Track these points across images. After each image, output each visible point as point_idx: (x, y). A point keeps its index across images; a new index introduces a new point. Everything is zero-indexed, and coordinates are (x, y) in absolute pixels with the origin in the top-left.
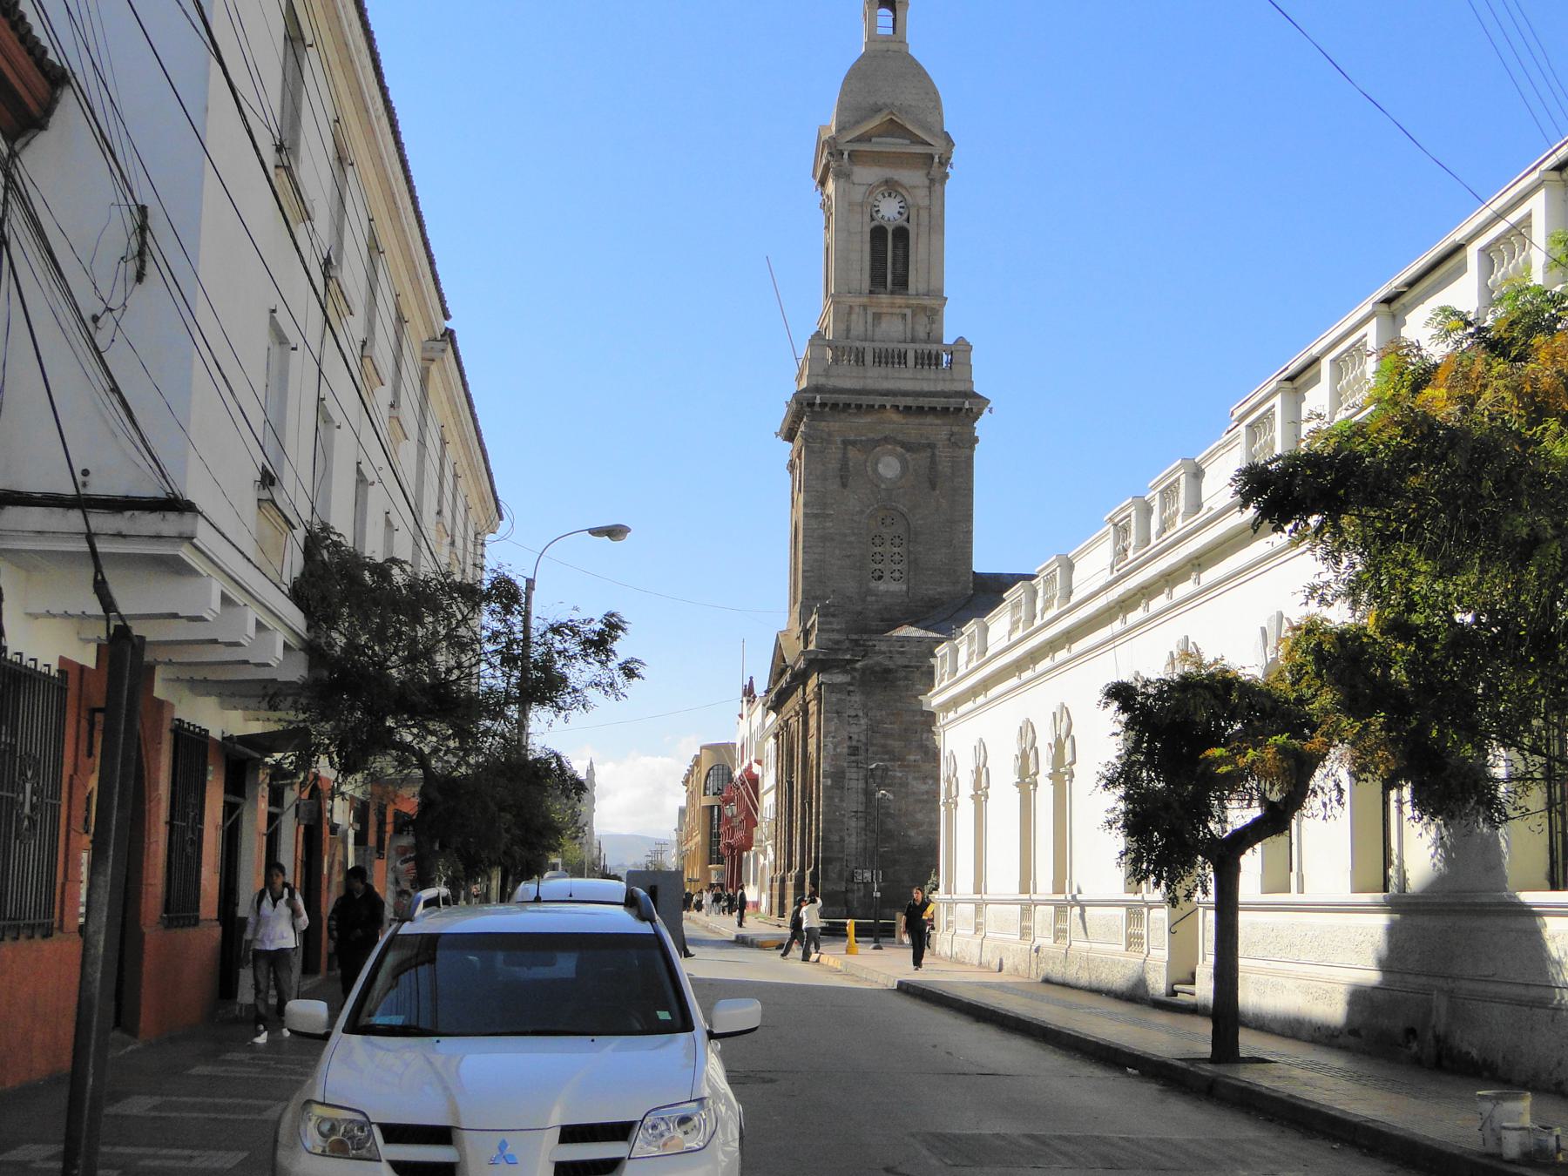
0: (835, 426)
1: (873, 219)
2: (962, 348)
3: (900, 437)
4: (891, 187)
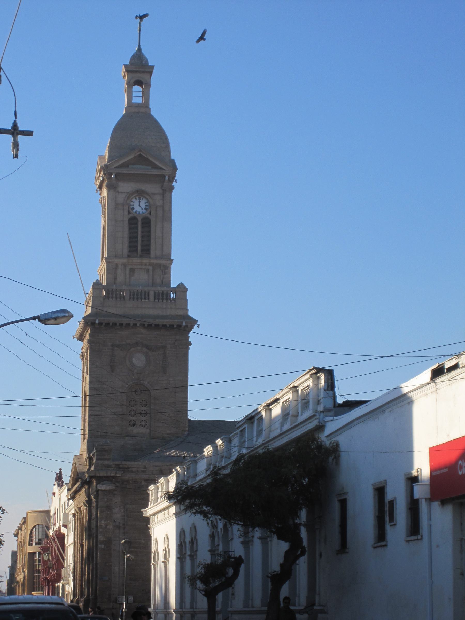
1: (129, 213)
2: (182, 289)
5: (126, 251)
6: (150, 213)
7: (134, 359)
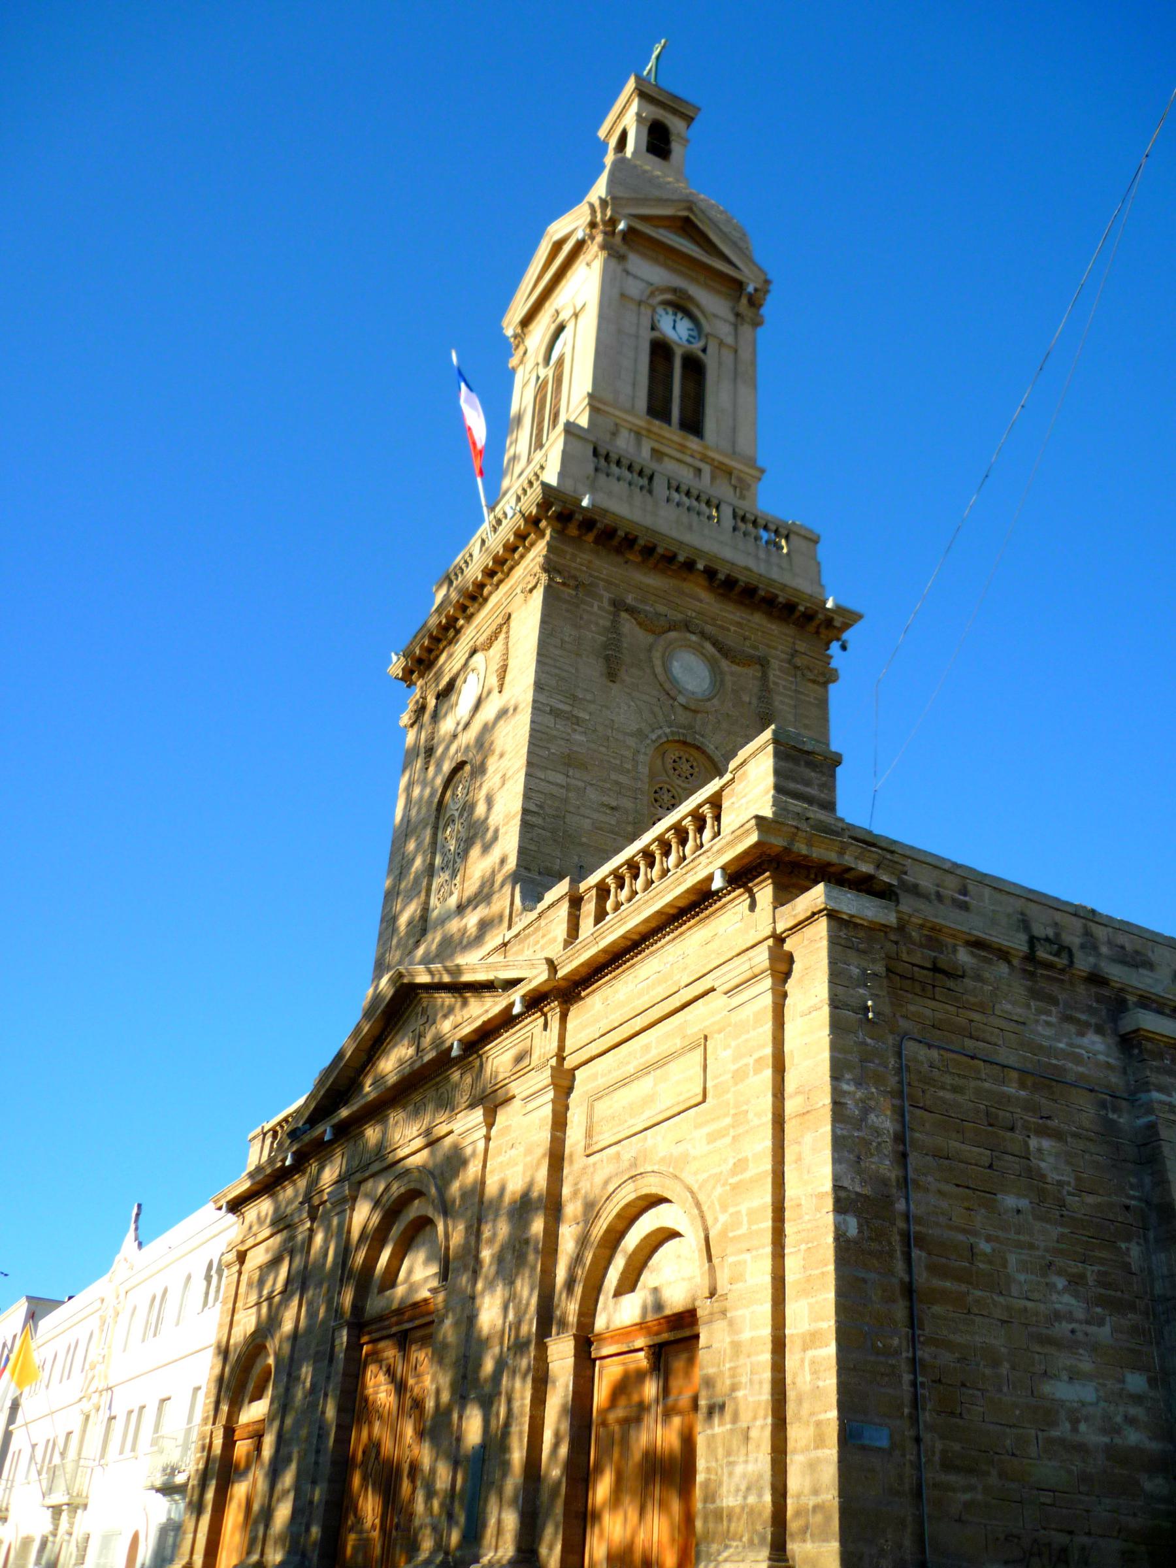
1: (653, 328)
3: (709, 629)
4: (681, 306)
5: (642, 403)
6: (704, 350)
7: (675, 664)
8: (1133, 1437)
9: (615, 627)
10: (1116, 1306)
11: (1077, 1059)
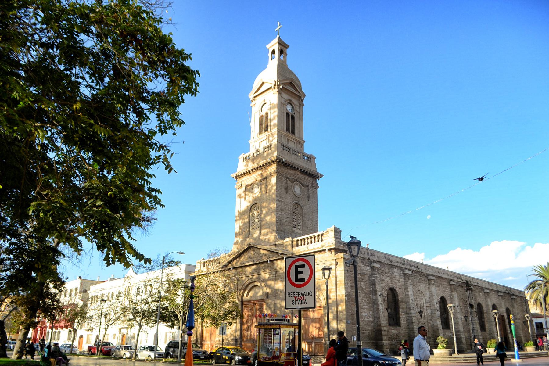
0: (285, 170)
3: (300, 180)
4: (290, 103)
8: (370, 319)
9: (286, 183)
10: (369, 303)
11: (366, 271)
